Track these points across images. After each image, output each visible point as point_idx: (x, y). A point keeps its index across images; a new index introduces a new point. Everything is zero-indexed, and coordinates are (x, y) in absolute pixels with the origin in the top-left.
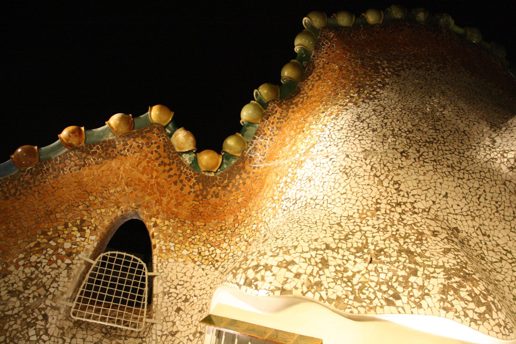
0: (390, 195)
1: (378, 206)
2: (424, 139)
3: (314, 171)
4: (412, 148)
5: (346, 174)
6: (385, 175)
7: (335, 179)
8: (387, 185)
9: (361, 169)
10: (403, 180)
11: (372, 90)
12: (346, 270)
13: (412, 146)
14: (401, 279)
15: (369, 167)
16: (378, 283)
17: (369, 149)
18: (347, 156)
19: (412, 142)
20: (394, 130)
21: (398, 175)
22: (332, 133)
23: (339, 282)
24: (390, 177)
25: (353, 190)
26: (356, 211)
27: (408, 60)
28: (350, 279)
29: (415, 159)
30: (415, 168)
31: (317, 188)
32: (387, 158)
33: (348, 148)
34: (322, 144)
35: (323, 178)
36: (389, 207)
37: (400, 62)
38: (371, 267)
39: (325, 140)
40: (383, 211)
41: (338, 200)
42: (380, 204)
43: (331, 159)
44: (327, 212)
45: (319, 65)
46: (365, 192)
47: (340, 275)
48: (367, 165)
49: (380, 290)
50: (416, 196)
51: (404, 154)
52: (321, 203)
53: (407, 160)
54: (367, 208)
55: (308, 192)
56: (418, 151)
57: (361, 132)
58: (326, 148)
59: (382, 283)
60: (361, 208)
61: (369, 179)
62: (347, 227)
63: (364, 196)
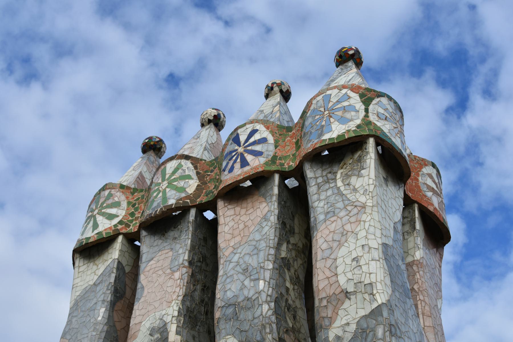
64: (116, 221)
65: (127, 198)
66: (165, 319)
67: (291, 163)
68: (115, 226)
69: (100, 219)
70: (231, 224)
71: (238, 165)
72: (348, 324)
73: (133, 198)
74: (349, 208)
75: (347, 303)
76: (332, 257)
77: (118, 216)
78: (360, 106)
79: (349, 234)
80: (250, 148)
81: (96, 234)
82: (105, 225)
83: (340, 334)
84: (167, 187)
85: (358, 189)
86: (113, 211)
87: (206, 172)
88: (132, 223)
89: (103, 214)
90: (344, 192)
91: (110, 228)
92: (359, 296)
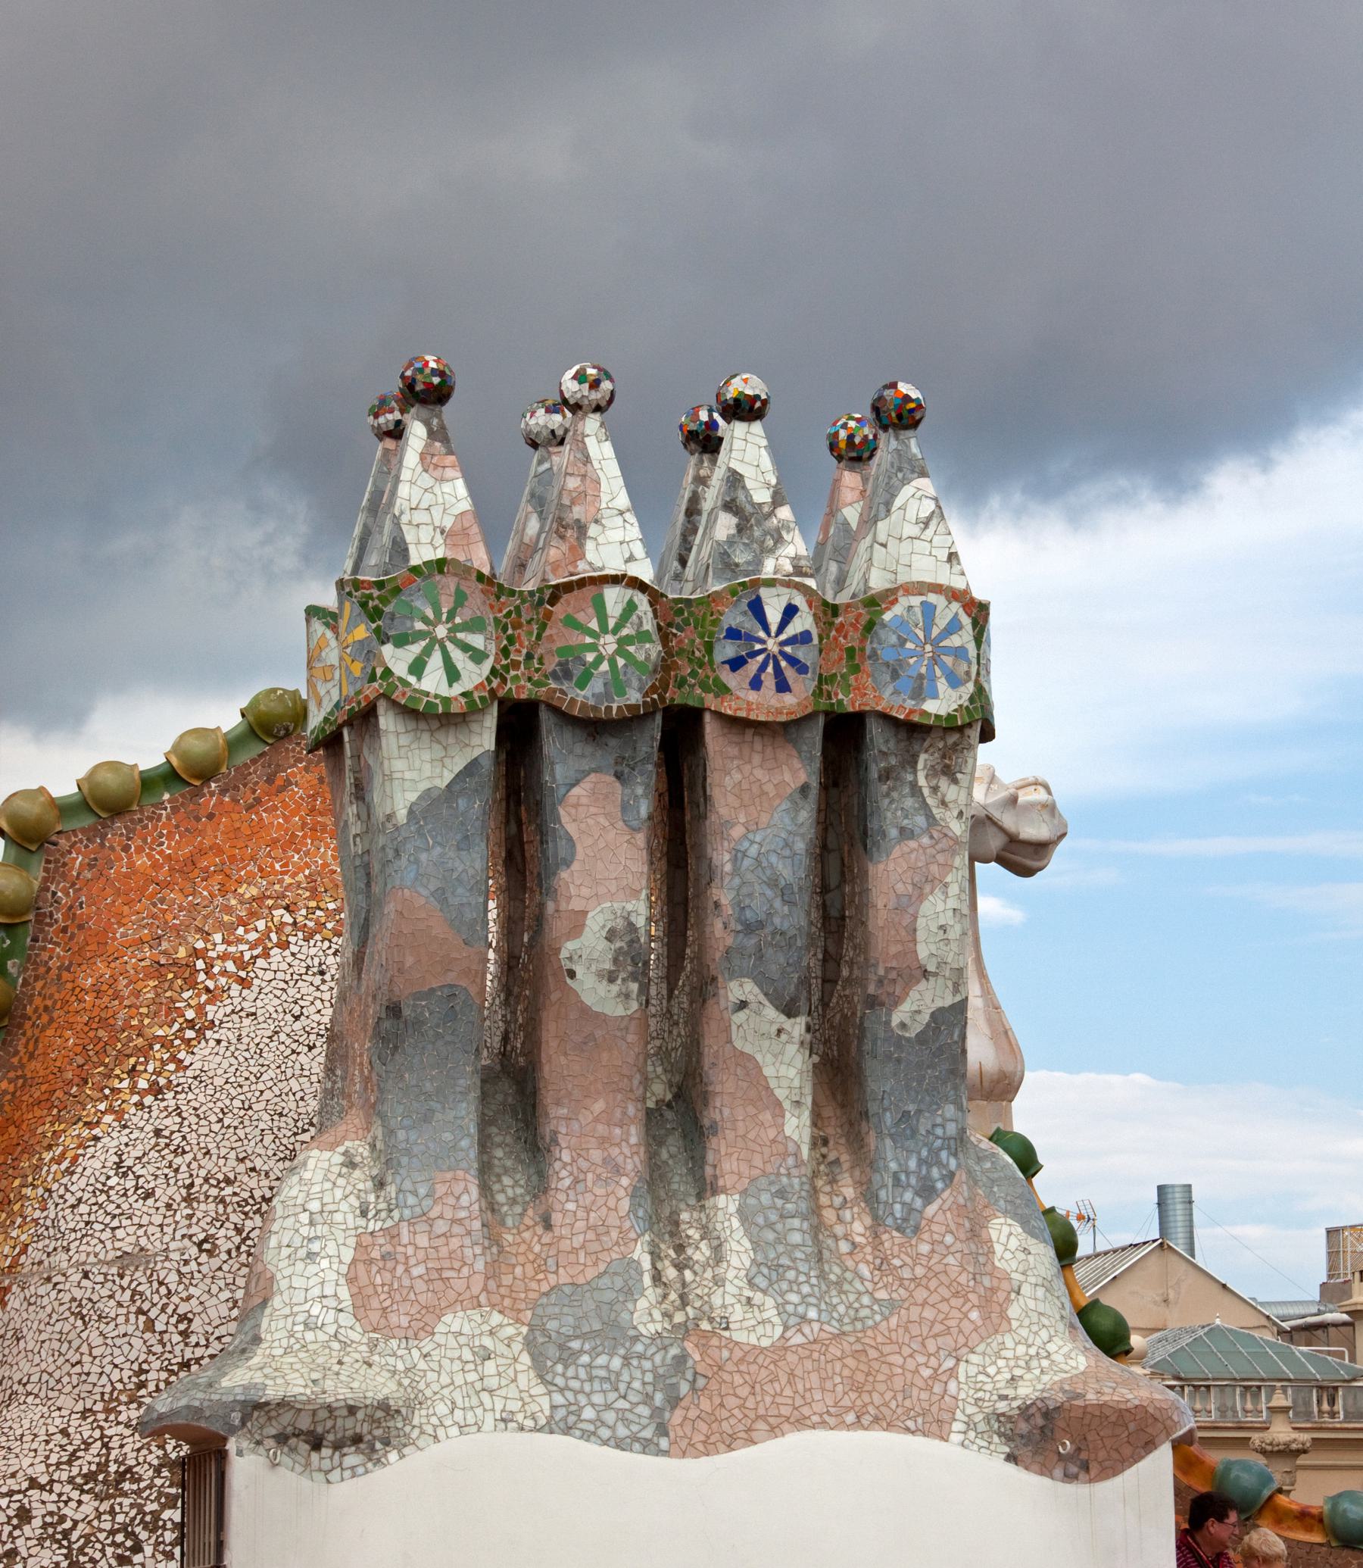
0: (168, 1348)
1: (143, 1378)
2: (257, 1194)
3: (25, 1315)
4: (227, 1225)
5: (83, 1318)
6: (159, 1306)
7: (61, 1333)
8: (164, 1328)
9: (112, 1303)
10: (200, 1309)
11: (166, 1056)
12: (62, 1519)
13: (228, 1219)
14: (148, 1518)
15: (128, 1293)
16: (112, 1532)
17: (129, 1249)
18: (86, 1276)
19: (230, 1209)
20: (192, 1185)
21: (189, 1298)
22: (60, 1214)
23: (47, 1543)
24: (169, 1310)
25: (95, 1352)
26: (98, 1397)
27: (287, 908)
28: (66, 1534)
29: (229, 1252)
30: (228, 1275)
31: (30, 1354)
32: (167, 1264)
33: (88, 1254)
34: (40, 1245)
35: (41, 1332)
36: (164, 1375)
37: (261, 925)
38: (105, 1506)
39: (46, 1233)
40: (152, 1387)
41: (66, 1379)
42: (147, 1372)
43: (56, 1284)
44: (45, 1409)
45: (50, 969)
46: (117, 1352)
47: (50, 1531)
48: (123, 1289)
49: (114, 1544)
50: (224, 1340)
51: (206, 1246)
52: (36, 1391)
53: (212, 1260)
54: (119, 1386)
55: (15, 1367)
56: (239, 1230)
57: (118, 1207)
58: (49, 1255)
59: (118, 1531)
60: (108, 1389)
61: (127, 1321)
62: (78, 1436)
63: (116, 1361)
64: (488, 665)
65: (492, 607)
66: (633, 919)
67: (841, 696)
68: (488, 679)
69: (458, 656)
70: (737, 777)
71: (768, 677)
72: (919, 1012)
73: (500, 611)
74: (936, 835)
75: (923, 985)
76: (911, 910)
77: (488, 656)
78: (971, 648)
79: (936, 882)
80: (788, 649)
81: (463, 694)
82: (473, 675)
83: (908, 1021)
84: (617, 652)
85: (951, 805)
86: (477, 641)
87: (670, 625)
88: (508, 672)
89: (465, 647)
90: (929, 801)
91: (482, 684)
92: (940, 980)
